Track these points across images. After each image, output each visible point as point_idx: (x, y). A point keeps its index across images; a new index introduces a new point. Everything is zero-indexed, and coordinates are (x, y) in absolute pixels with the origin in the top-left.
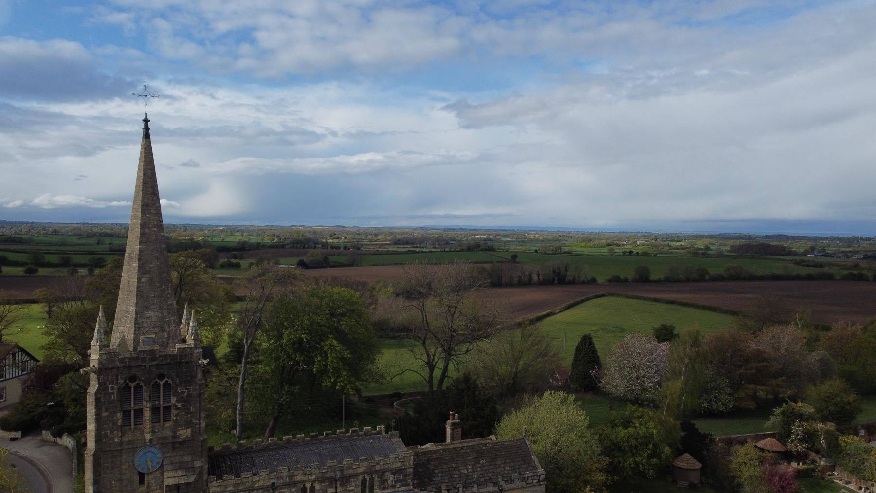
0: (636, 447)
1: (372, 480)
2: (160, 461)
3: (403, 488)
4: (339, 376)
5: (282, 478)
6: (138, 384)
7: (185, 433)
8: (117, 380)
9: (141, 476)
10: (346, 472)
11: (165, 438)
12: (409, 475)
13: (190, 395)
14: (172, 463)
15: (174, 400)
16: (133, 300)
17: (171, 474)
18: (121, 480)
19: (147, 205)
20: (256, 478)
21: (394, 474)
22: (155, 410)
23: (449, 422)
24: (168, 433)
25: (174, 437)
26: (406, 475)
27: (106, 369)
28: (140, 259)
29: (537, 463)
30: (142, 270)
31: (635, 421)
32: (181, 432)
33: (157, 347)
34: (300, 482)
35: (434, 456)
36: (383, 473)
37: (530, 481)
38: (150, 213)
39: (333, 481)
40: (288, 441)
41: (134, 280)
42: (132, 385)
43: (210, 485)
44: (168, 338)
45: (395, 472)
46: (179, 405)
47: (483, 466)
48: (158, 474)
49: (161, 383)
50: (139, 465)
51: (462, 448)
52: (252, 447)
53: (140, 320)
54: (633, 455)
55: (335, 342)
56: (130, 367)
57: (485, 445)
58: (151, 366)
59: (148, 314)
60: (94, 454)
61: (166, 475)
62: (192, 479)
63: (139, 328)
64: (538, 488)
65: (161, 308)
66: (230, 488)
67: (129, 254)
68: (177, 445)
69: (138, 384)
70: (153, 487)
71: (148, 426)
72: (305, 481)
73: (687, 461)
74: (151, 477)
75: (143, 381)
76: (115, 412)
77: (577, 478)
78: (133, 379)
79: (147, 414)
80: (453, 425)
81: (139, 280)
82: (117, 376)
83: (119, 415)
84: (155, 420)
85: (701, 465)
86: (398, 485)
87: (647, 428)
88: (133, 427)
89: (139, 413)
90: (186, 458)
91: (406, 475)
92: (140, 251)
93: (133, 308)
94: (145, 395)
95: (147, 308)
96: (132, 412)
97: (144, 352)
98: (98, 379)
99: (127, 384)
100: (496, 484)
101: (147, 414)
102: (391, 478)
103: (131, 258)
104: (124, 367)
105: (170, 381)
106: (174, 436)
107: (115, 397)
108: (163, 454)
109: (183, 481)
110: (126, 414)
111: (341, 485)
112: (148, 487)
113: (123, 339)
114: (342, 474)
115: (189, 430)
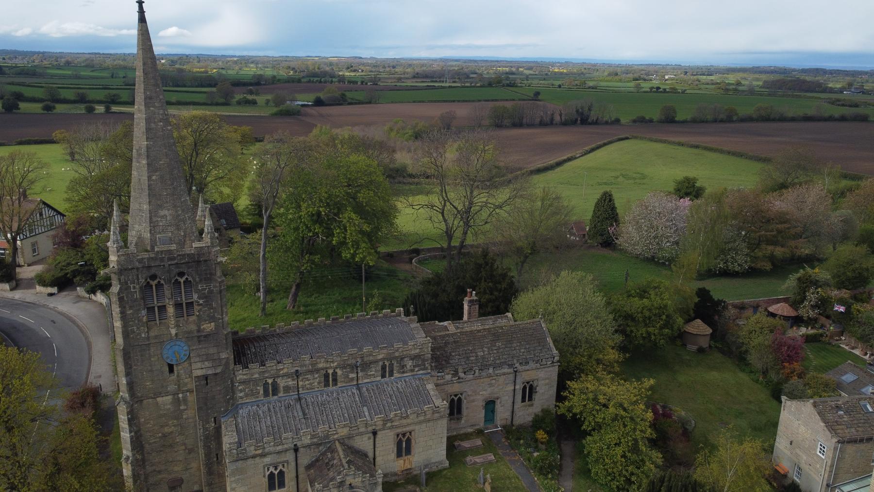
0: (650, 318)
1: (391, 365)
2: (188, 353)
3: (421, 372)
4: (358, 248)
5: (305, 365)
6: (159, 282)
7: (209, 327)
8: (138, 279)
9: (171, 368)
10: (366, 359)
11: (190, 332)
12: (427, 360)
13: (211, 292)
14: (199, 356)
15: (195, 297)
16: (146, 199)
17: (199, 365)
18: (151, 371)
19: (150, 98)
20: (280, 366)
21: (412, 359)
22: (178, 306)
23: (467, 299)
24: (193, 327)
25: (199, 331)
26: (424, 360)
27: (126, 270)
28: (148, 157)
29: (552, 345)
30: (152, 167)
31: (652, 292)
32: (205, 326)
33: (173, 247)
34: (322, 369)
35: (451, 340)
36: (402, 359)
37: (544, 362)
38: (154, 107)
39: (354, 368)
40: (310, 324)
41: (145, 178)
42: (154, 283)
43: (236, 373)
44: (185, 236)
45: (413, 358)
46: (201, 302)
47: (499, 348)
48: (186, 364)
49: (182, 280)
50: (168, 358)
51: (479, 331)
52: (275, 331)
53: (154, 219)
54: (646, 325)
55: (353, 216)
56: (149, 267)
57: (501, 328)
60: (124, 349)
61: (194, 366)
62: (219, 370)
63: (154, 227)
64: (551, 369)
65: (175, 206)
66: (257, 376)
67: (137, 151)
68: (203, 338)
69: (159, 282)
70: (183, 376)
71: (172, 321)
72: (327, 368)
73: (699, 328)
75: (164, 279)
76: (139, 310)
77: (590, 357)
78: (153, 277)
79: (171, 310)
80: (470, 301)
81: (149, 178)
83: (144, 312)
84: (179, 315)
85: (711, 331)
86: (416, 369)
87: (662, 299)
88: (158, 322)
89: (163, 309)
90: (212, 351)
91: (424, 360)
92: (148, 148)
93: (146, 207)
95: (161, 207)
96: (156, 309)
97: (162, 252)
98: (119, 280)
100: (511, 366)
101: (171, 310)
102: (409, 364)
103: (139, 155)
104: (143, 267)
105: (190, 279)
107: (138, 295)
108: (189, 346)
109: (210, 372)
110: (151, 310)
111: (362, 371)
112: (178, 376)
113: (140, 238)
114: (363, 361)
115: (213, 324)
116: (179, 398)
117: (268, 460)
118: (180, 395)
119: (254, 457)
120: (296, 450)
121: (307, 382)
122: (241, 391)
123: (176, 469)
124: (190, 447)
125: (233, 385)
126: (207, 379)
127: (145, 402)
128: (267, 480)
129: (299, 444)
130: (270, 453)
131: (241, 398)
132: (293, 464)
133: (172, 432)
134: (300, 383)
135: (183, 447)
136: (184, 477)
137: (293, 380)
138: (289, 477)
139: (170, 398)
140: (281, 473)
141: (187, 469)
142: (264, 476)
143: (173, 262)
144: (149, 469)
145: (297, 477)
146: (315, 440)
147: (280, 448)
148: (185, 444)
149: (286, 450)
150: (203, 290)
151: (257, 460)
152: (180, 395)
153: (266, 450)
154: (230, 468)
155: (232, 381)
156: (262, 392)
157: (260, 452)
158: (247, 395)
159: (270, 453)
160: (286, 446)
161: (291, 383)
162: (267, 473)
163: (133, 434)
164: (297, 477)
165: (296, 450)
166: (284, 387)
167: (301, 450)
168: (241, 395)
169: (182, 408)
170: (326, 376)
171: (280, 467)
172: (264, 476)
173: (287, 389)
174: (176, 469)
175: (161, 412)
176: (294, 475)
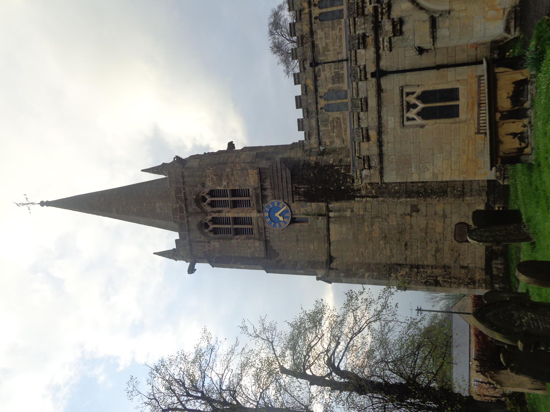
8: (201, 242)
22: (235, 205)
49: (209, 199)
59: (158, 211)
72: (311, 17)
74: (297, 211)
84: (248, 204)
89: (236, 221)
94: (216, 215)
99: (211, 231)
105: (207, 190)
110: (237, 232)
115: (250, 171)
116: (335, 217)
117: (391, 121)
118: (331, 214)
119: (380, 144)
120: (379, 74)
123: (439, 229)
124: (409, 210)
129: (371, 68)
130: (380, 117)
132: (410, 77)
133: (381, 229)
134: (331, 57)
135: (408, 217)
136: (456, 219)
138: (432, 81)
139: (332, 226)
140: (425, 97)
141: (445, 216)
142: (422, 126)
143: (184, 209)
144: (430, 261)
145: (438, 67)
146: (370, 40)
147: (372, 102)
148: (404, 215)
149: (379, 90)
150: (212, 181)
151: (384, 138)
154: (391, 177)
156: (337, 114)
157: (373, 134)
159: (380, 117)
162: (419, 121)
167: (384, 64)
170: (322, 18)
171: (412, 99)
172: (422, 126)
174: (439, 229)
176: (433, 72)
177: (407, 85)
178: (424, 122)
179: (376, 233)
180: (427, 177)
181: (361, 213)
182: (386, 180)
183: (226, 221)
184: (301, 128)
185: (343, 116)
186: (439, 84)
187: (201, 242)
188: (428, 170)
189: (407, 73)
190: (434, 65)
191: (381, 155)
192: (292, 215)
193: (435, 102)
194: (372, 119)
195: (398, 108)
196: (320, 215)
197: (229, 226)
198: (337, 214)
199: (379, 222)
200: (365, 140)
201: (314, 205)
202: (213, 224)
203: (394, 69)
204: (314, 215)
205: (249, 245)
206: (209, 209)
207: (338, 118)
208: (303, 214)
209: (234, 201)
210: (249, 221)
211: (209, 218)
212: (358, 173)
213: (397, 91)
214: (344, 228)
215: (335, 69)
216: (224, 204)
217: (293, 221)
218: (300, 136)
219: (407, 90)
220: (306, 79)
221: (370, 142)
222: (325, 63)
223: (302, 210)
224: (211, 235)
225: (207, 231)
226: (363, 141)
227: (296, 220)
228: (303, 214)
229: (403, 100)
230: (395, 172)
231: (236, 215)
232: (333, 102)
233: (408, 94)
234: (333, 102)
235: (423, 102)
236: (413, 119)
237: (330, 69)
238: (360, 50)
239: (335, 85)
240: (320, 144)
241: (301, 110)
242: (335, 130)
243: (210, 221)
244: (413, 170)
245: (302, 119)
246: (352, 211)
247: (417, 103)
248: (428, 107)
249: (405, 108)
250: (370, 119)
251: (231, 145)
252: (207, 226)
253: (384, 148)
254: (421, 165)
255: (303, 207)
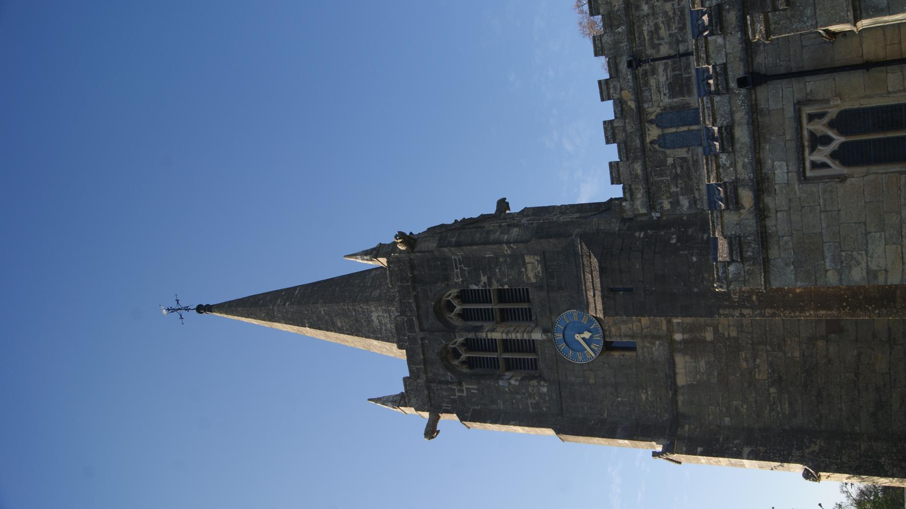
8: (447, 383)
22: (506, 317)
32: (531, 275)
43: (629, 214)
46: (484, 279)
56: (425, 361)
58: (422, 330)
81: (340, 331)
82: (441, 382)
84: (526, 316)
89: (508, 345)
95: (370, 321)
99: (463, 363)
104: (426, 372)
105: (454, 291)
106: (539, 287)
109: (597, 281)
110: (511, 365)
112: (633, 337)
115: (528, 259)
116: (684, 341)
117: (781, 171)
118: (678, 337)
119: (761, 212)
120: (752, 80)
121: (663, 32)
122: (676, 203)
125: (656, 225)
126: (612, 290)
127: (682, 409)
128: (859, 170)
130: (758, 163)
131: (694, 202)
132: (813, 85)
137: (654, 72)
139: (679, 360)
140: (844, 122)
142: (842, 179)
143: (416, 324)
145: (867, 65)
147: (742, 134)
149: (754, 110)
150: (463, 276)
151: (768, 200)
152: (678, 337)
153: (745, 174)
154: (786, 278)
155: (642, 227)
157: (746, 197)
158: (688, 190)
159: (758, 163)
160: (741, 116)
161: (661, 76)
162: (836, 168)
163: (747, 450)
164: (867, 65)
165: (752, 80)
166: (673, 95)
168: (685, 202)
169: (709, 336)
171: (820, 127)
173: (678, 86)
175: (714, 380)
177: (808, 102)
178: (845, 171)
179: (762, 375)
180: (857, 275)
181: (734, 334)
182: (775, 285)
183: (491, 345)
184: (615, 180)
185: (692, 156)
186: (870, 97)
187: (447, 383)
188: (858, 264)
189: (808, 78)
190: (860, 61)
191: (764, 238)
192: (604, 337)
193: (865, 132)
194: (744, 166)
195: (792, 145)
196: (658, 337)
197: (494, 355)
198: (686, 336)
199: (767, 350)
200: (731, 207)
201: (645, 320)
202: (466, 351)
203: (783, 71)
204: (646, 336)
205: (530, 389)
206: (459, 323)
207: (684, 160)
208: (626, 336)
209: (502, 310)
210: (530, 346)
211: (460, 340)
212: (721, 271)
213: (790, 112)
214: (702, 363)
215: (673, 70)
216: (487, 316)
217: (608, 347)
218: (617, 191)
219: (808, 110)
220: (622, 89)
221: (742, 211)
222: (654, 60)
223: (623, 328)
224: (465, 370)
225: (456, 362)
226: (727, 208)
227: (613, 345)
228: (626, 336)
229: (801, 128)
230: (792, 267)
231: (504, 337)
232: (673, 130)
233: (811, 117)
234: (673, 130)
235: (842, 133)
236: (824, 165)
237: (665, 70)
238: (714, 38)
239: (675, 100)
240: (651, 207)
241: (614, 146)
242: (679, 181)
243: (462, 344)
244: (827, 264)
245: (617, 162)
246: (716, 330)
247: (831, 133)
248: (852, 142)
249: (806, 144)
250: (739, 166)
251: (503, 204)
252: (457, 355)
253: (770, 223)
254: (843, 254)
255: (625, 322)
